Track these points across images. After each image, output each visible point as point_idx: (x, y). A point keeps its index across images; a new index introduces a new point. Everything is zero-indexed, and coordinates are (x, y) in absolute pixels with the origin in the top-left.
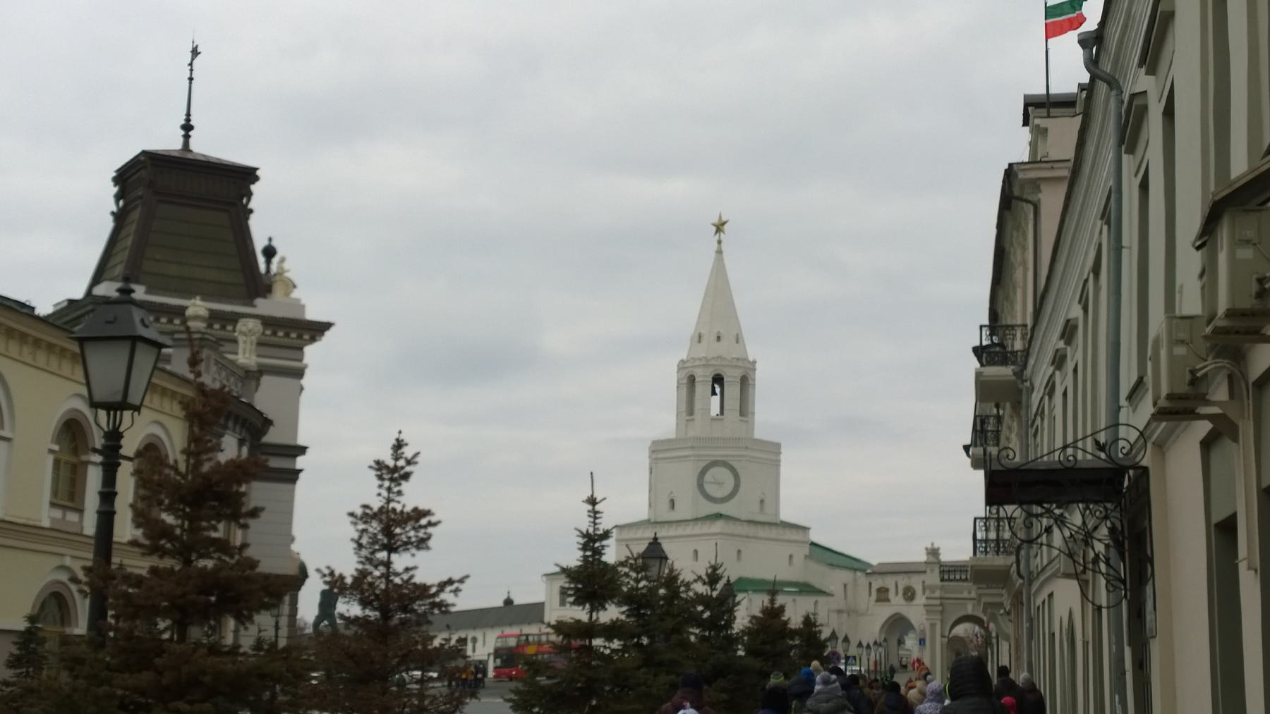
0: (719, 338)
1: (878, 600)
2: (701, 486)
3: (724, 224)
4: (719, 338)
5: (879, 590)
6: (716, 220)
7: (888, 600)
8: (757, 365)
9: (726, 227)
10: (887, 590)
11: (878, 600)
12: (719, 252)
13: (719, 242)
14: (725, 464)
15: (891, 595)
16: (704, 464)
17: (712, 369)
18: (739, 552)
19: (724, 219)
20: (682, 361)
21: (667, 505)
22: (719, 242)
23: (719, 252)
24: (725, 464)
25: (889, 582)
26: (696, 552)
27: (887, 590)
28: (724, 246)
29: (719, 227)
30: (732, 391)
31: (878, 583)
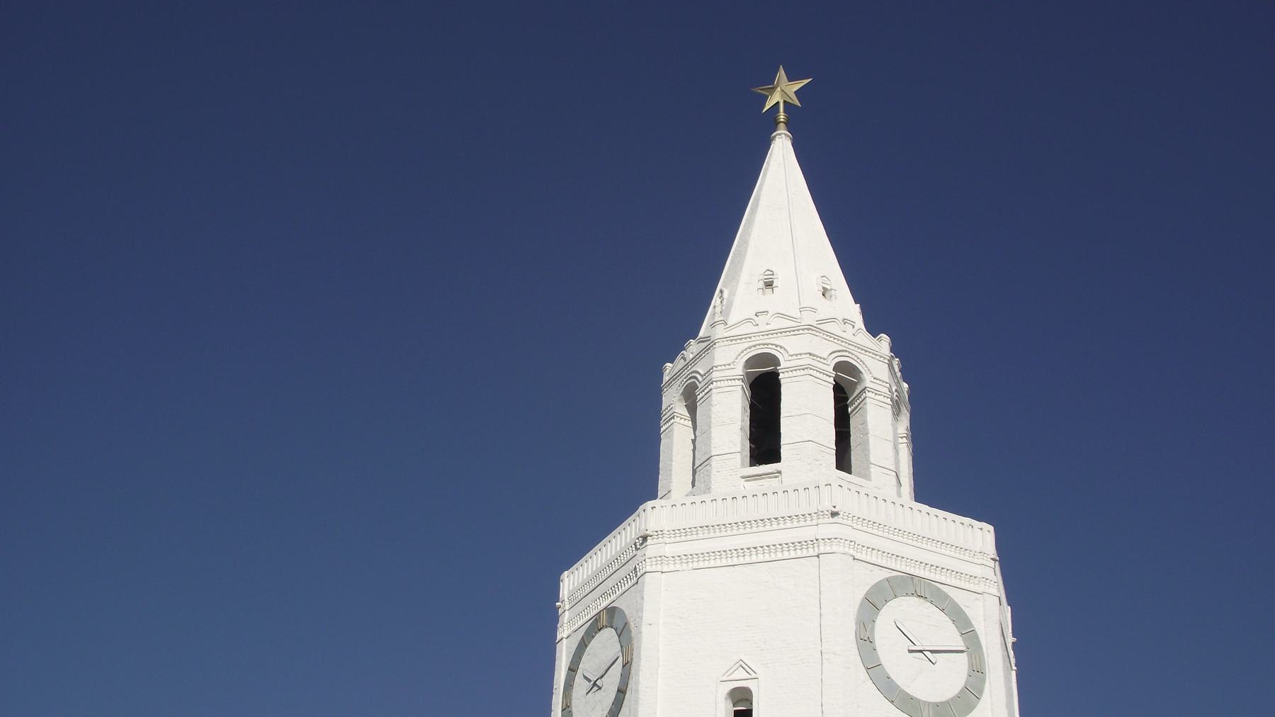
4: (825, 293)
16: (870, 578)
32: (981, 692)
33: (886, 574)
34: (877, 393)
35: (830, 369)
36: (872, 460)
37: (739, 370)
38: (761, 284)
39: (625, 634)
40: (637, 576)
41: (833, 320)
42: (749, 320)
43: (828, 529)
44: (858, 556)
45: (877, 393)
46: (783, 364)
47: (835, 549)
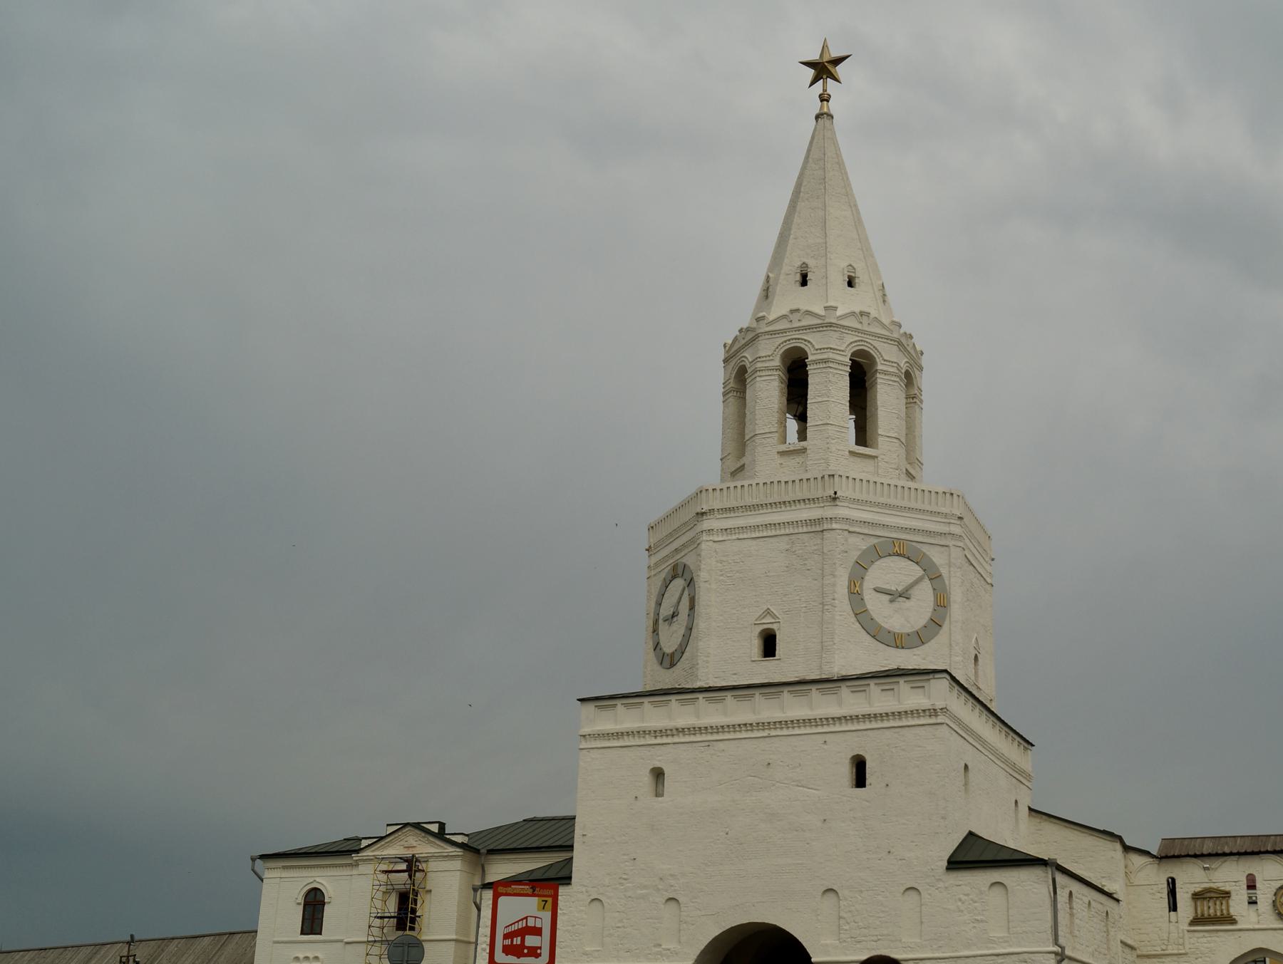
1: (1196, 921)
3: (837, 61)
4: (850, 284)
5: (1197, 896)
7: (1232, 921)
9: (840, 70)
10: (1226, 895)
11: (1196, 921)
13: (824, 98)
15: (1238, 905)
17: (850, 338)
19: (835, 53)
22: (824, 98)
25: (1229, 875)
27: (1226, 895)
28: (833, 106)
30: (886, 395)
31: (1191, 878)
33: (875, 541)
34: (885, 373)
35: (847, 360)
36: (880, 432)
37: (777, 362)
38: (798, 277)
39: (691, 583)
40: (694, 543)
41: (853, 314)
42: (784, 317)
43: (830, 512)
44: (851, 529)
45: (885, 373)
46: (811, 358)
47: (834, 526)
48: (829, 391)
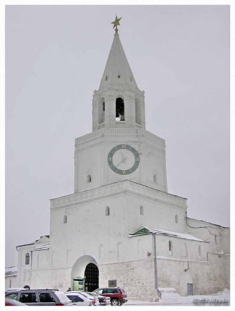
0: (119, 77)
2: (110, 163)
4: (119, 77)
6: (114, 20)
8: (145, 95)
12: (117, 35)
13: (117, 30)
14: (128, 147)
18: (141, 208)
20: (95, 91)
21: (86, 179)
22: (117, 30)
23: (117, 35)
24: (128, 147)
26: (108, 209)
29: (116, 23)
32: (138, 166)
48: (112, 107)
